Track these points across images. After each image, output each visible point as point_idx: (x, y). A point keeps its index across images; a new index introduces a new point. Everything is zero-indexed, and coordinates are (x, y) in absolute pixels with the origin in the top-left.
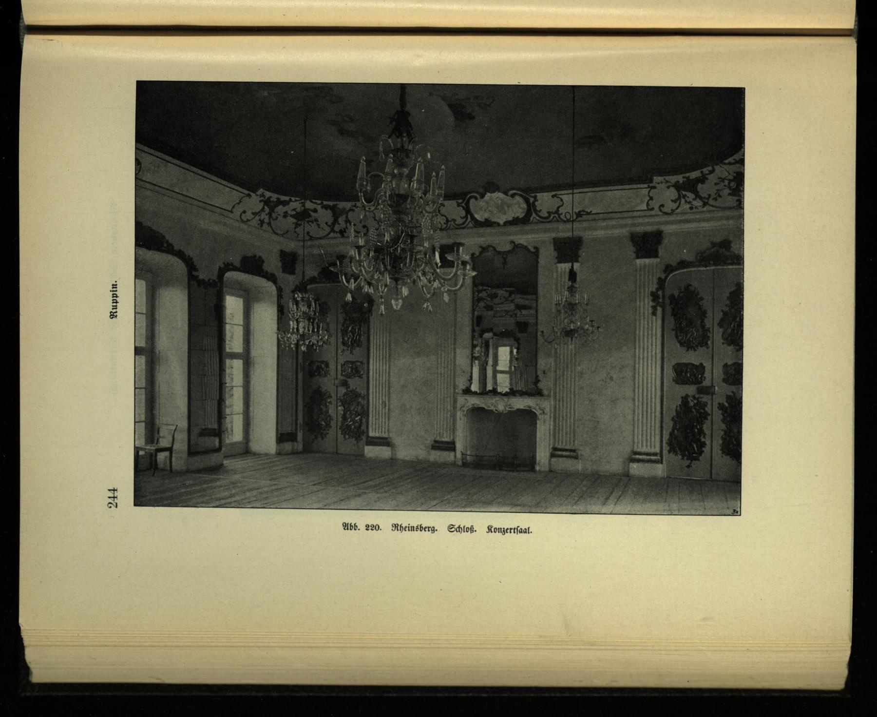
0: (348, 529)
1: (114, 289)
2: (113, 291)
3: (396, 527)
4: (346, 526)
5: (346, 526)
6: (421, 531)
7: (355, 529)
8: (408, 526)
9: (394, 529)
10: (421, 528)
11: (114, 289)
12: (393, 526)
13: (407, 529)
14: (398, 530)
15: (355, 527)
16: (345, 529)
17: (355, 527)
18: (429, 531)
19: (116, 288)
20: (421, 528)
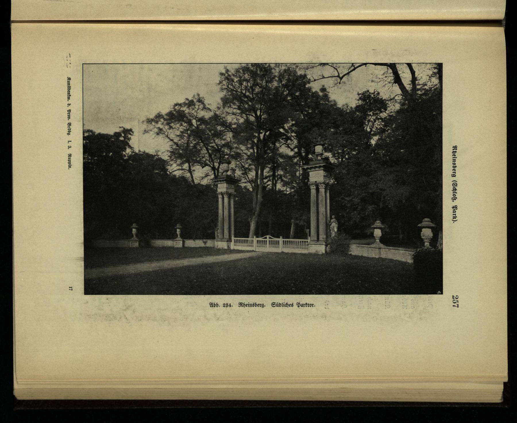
0: (213, 306)
1: (454, 159)
2: (455, 158)
3: (241, 304)
4: (212, 305)
5: (212, 305)
6: (256, 306)
7: (217, 307)
8: (248, 303)
9: (240, 305)
10: (255, 305)
11: (454, 159)
12: (239, 304)
13: (247, 306)
14: (242, 306)
15: (217, 305)
16: (211, 307)
17: (217, 305)
18: (260, 306)
19: (453, 160)
20: (255, 305)
